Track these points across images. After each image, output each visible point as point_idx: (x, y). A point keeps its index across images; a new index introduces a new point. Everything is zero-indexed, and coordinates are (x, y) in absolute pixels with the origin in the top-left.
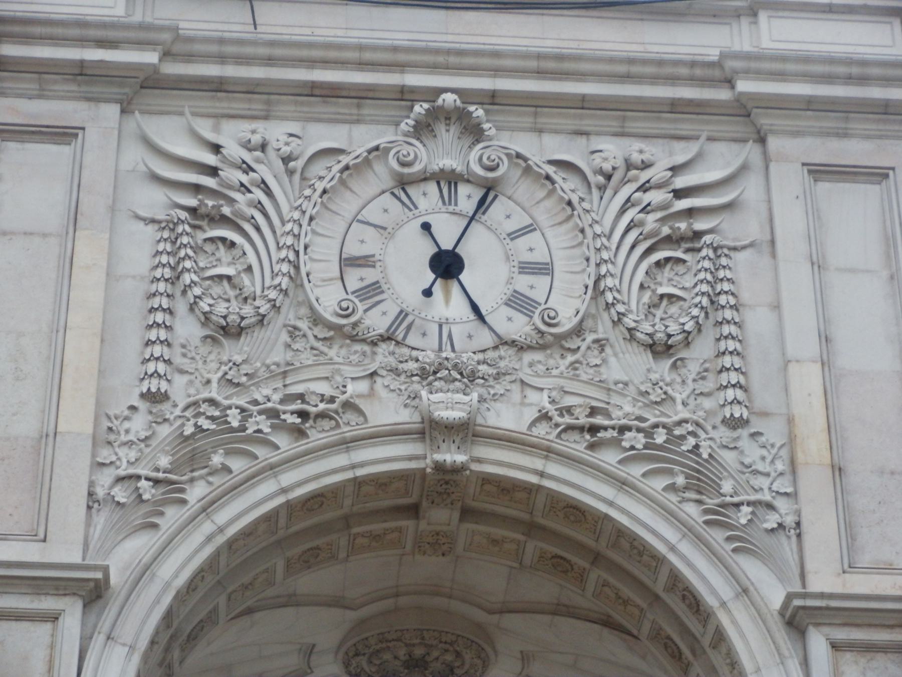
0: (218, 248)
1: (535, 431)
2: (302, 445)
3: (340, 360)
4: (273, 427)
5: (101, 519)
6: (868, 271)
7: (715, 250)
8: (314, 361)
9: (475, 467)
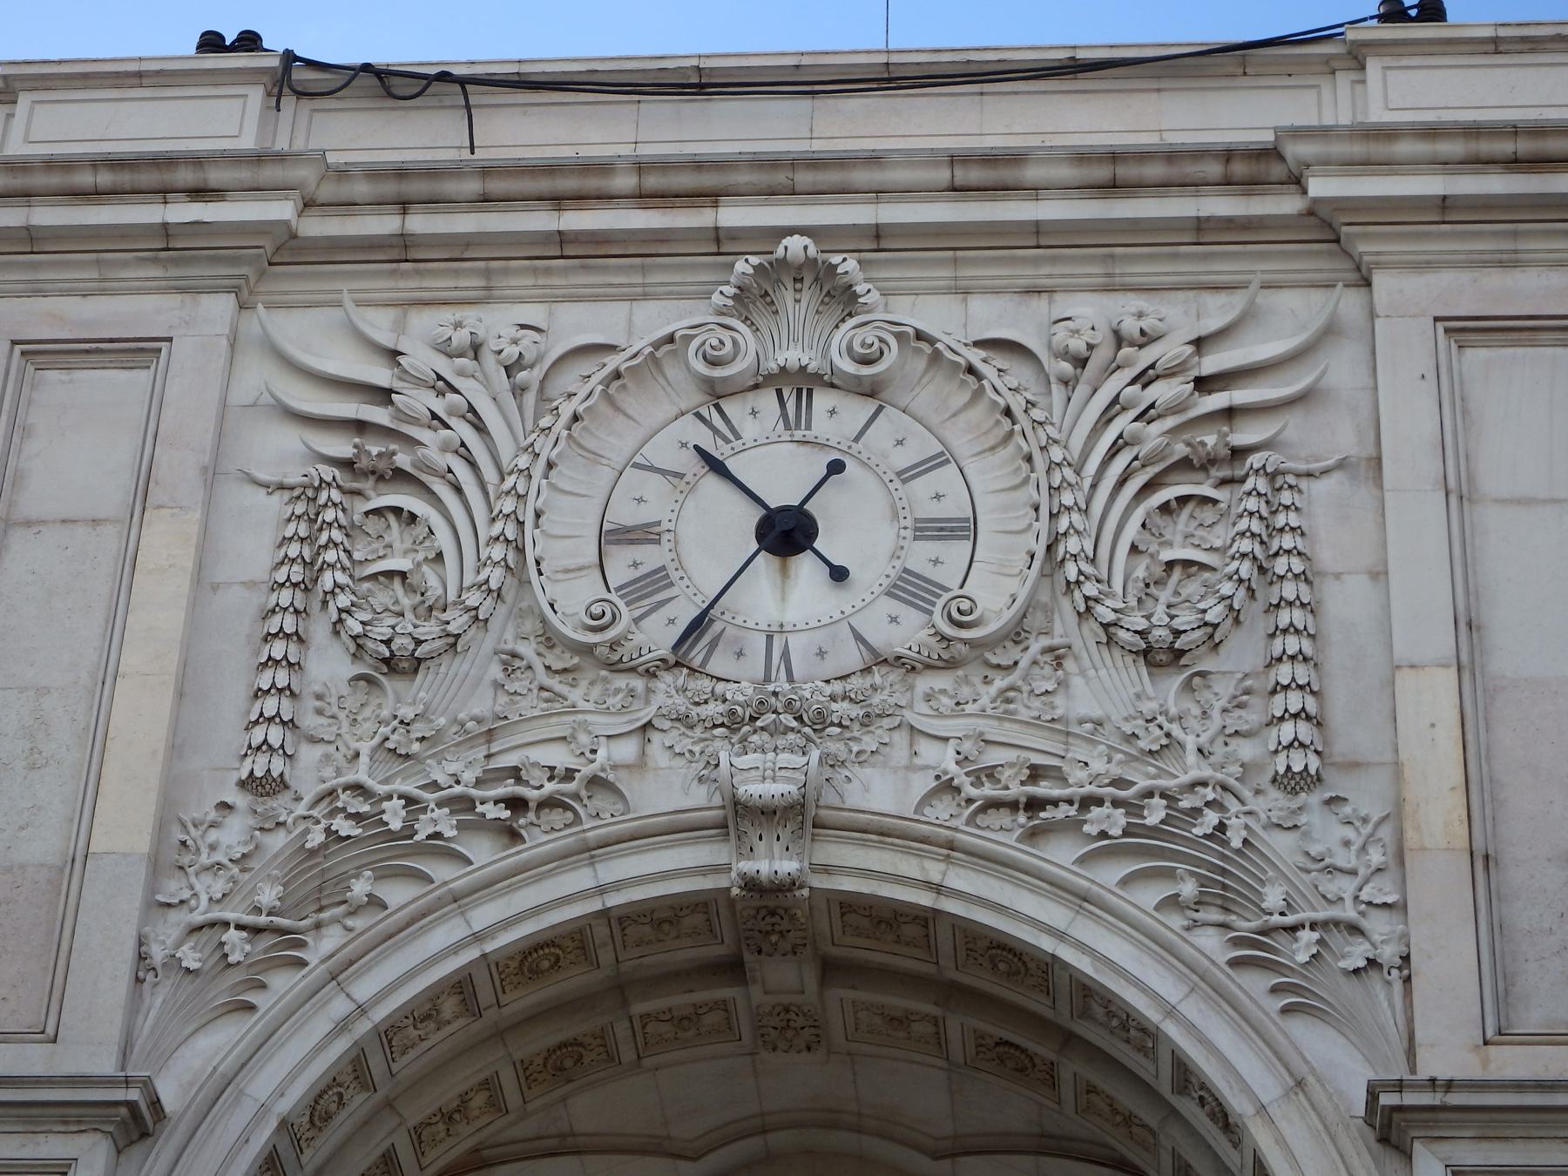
4: (461, 826)
5: (157, 999)
6: (1554, 501)
7: (1272, 477)
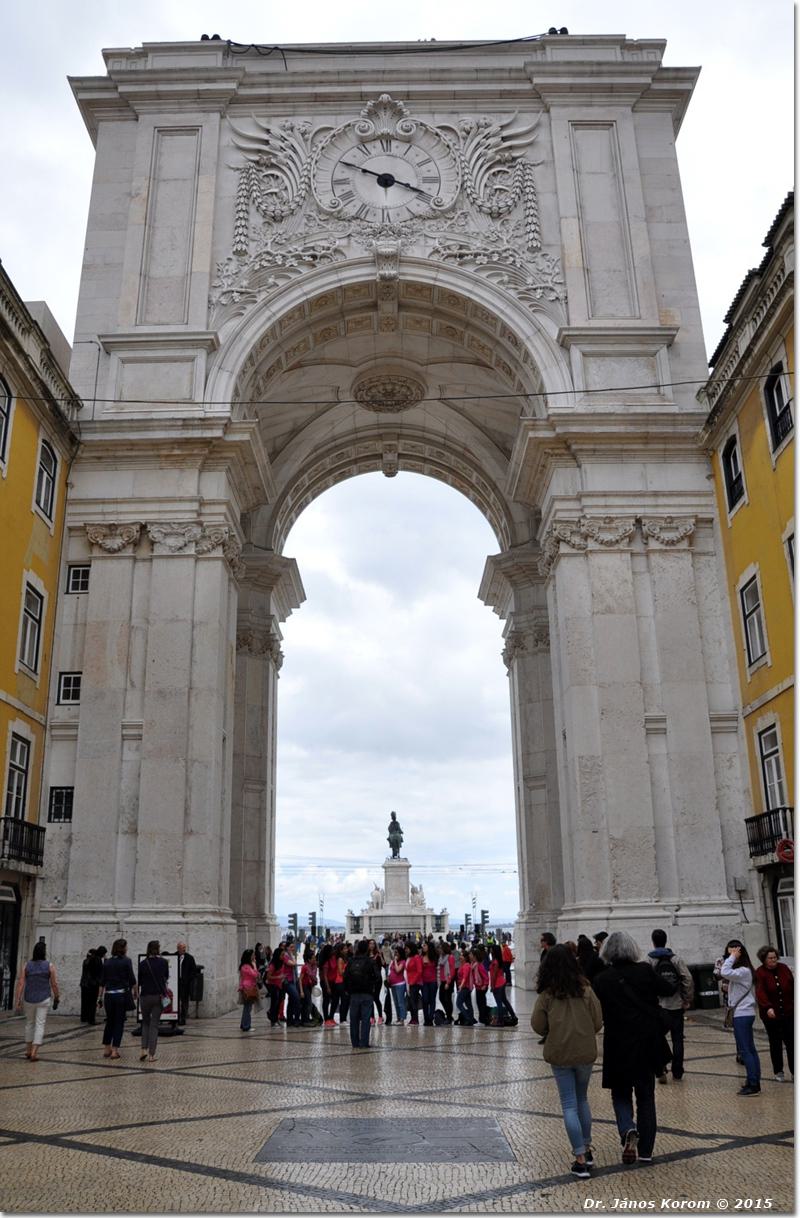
2: (314, 271)
5: (215, 313)
9: (401, 277)
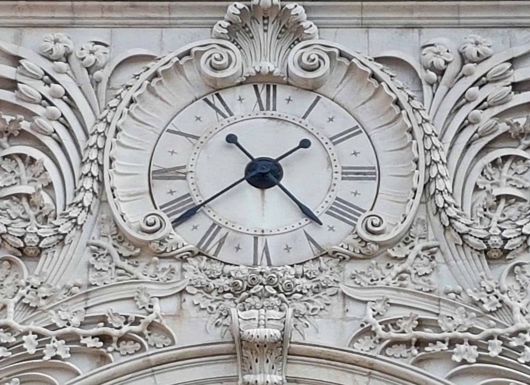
0: (17, 166)
1: (357, 347)
3: (147, 279)
8: (119, 281)
